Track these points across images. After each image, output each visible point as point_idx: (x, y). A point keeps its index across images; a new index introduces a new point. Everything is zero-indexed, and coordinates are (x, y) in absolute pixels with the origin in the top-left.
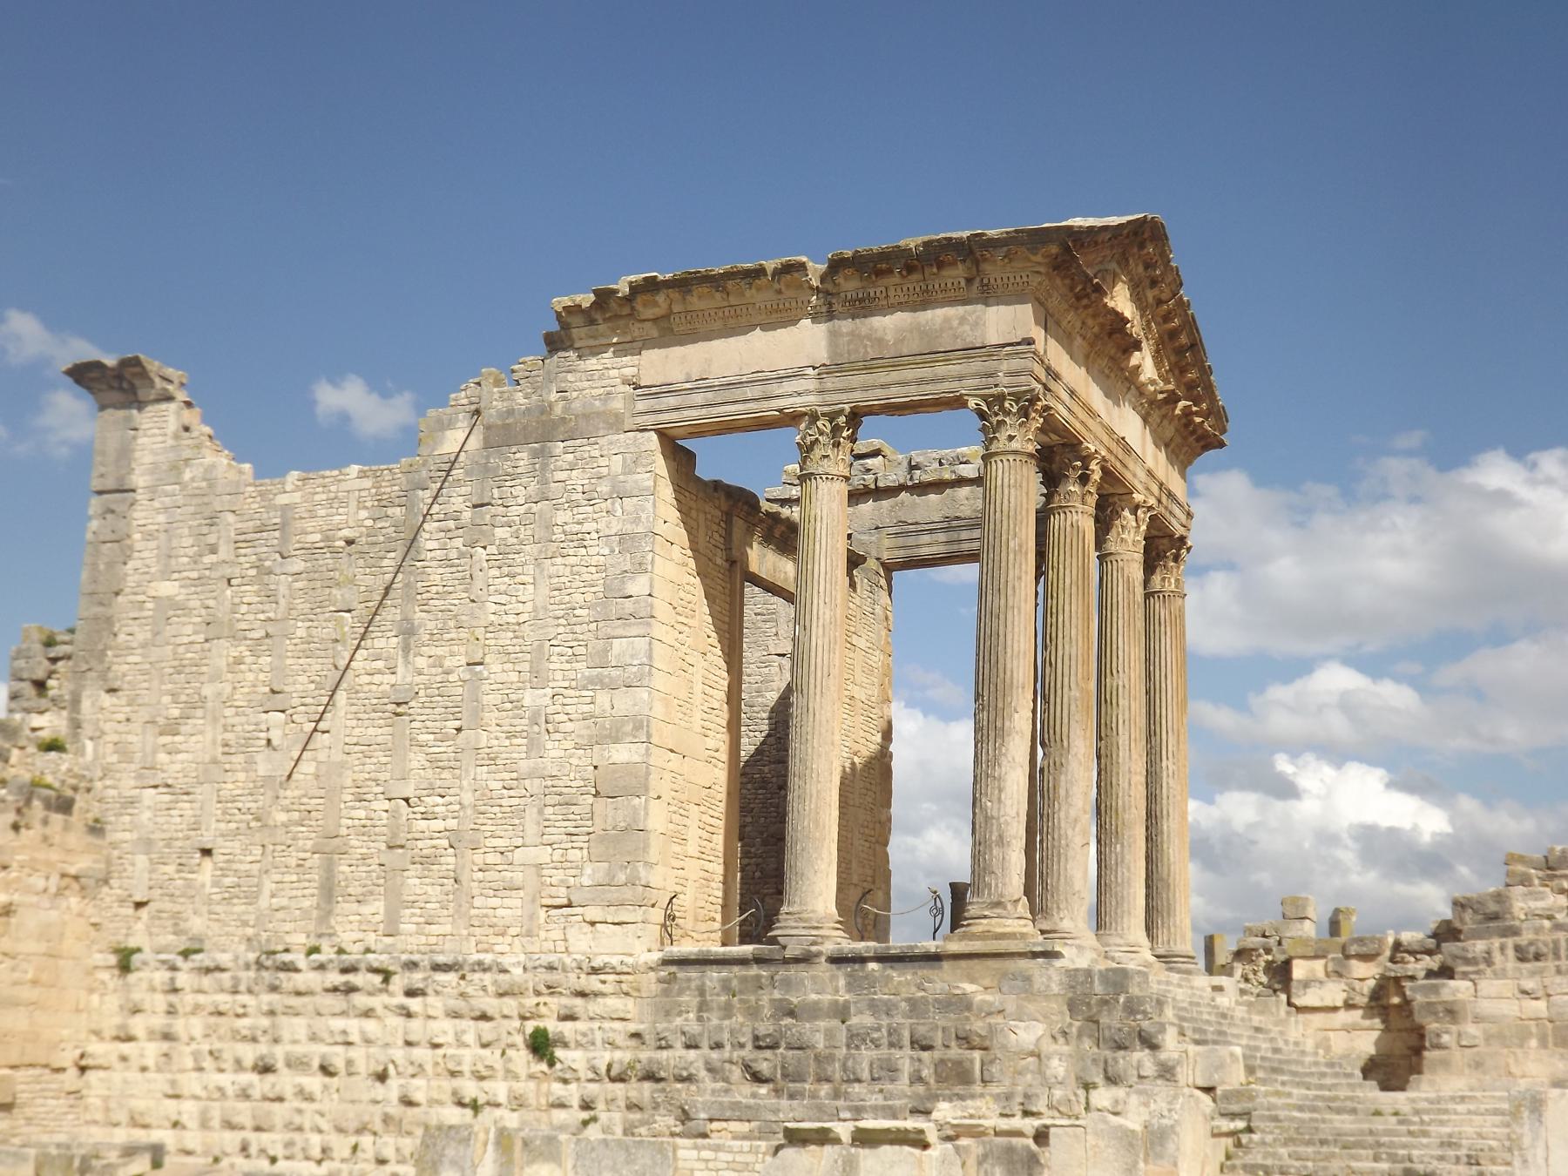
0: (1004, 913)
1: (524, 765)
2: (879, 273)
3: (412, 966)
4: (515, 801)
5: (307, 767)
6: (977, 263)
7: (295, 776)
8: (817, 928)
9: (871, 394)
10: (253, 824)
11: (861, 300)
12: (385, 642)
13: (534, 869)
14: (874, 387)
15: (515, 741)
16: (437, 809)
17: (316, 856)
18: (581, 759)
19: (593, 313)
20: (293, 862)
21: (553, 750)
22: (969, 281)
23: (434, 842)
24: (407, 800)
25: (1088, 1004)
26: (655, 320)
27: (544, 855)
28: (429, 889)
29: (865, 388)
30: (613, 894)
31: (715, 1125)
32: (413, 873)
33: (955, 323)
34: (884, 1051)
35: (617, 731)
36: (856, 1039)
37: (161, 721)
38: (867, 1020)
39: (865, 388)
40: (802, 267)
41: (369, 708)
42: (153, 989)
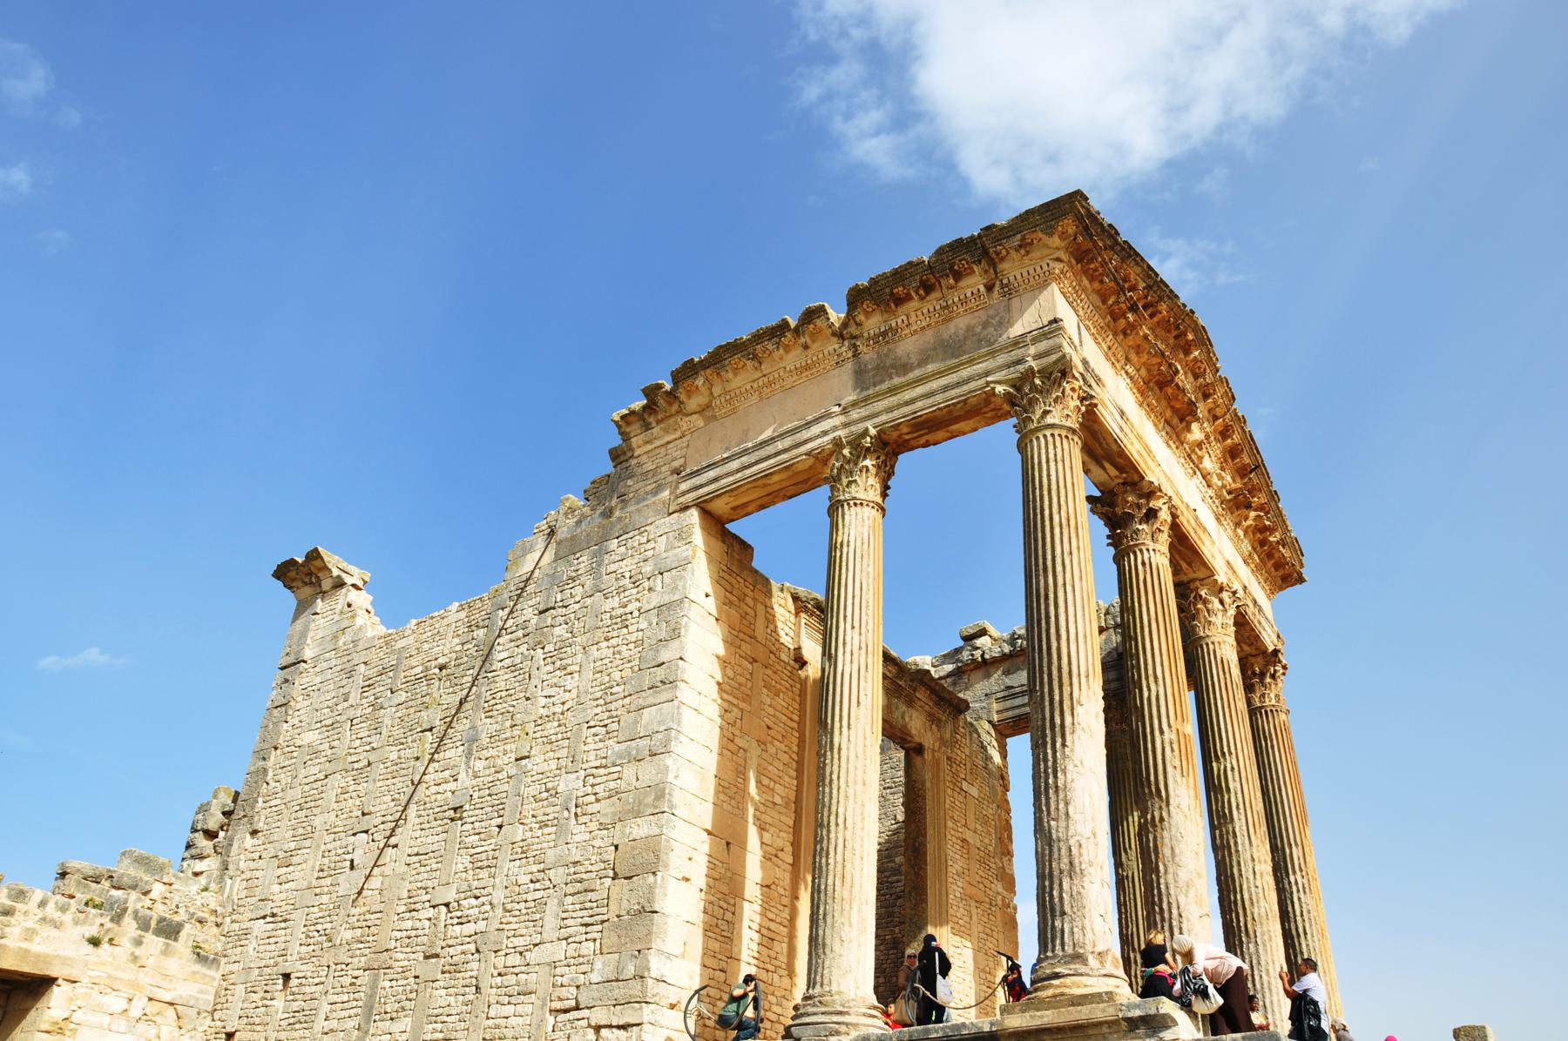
0: (1082, 969)
1: (551, 855)
2: (900, 301)
4: (538, 895)
5: (375, 883)
6: (993, 264)
7: (365, 893)
8: (841, 1013)
9: (896, 414)
10: (325, 945)
11: (884, 334)
12: (453, 754)
13: (547, 968)
14: (899, 406)
15: (546, 830)
16: (471, 912)
17: (367, 972)
18: (603, 840)
19: (646, 416)
20: (347, 980)
21: (579, 833)
22: (989, 288)
23: (464, 947)
24: (447, 905)
26: (701, 411)
27: (559, 951)
28: (452, 999)
29: (889, 410)
30: (619, 991)
32: (442, 984)
33: (978, 330)
35: (640, 803)
37: (281, 855)
39: (889, 410)
40: (821, 311)
41: (431, 818)
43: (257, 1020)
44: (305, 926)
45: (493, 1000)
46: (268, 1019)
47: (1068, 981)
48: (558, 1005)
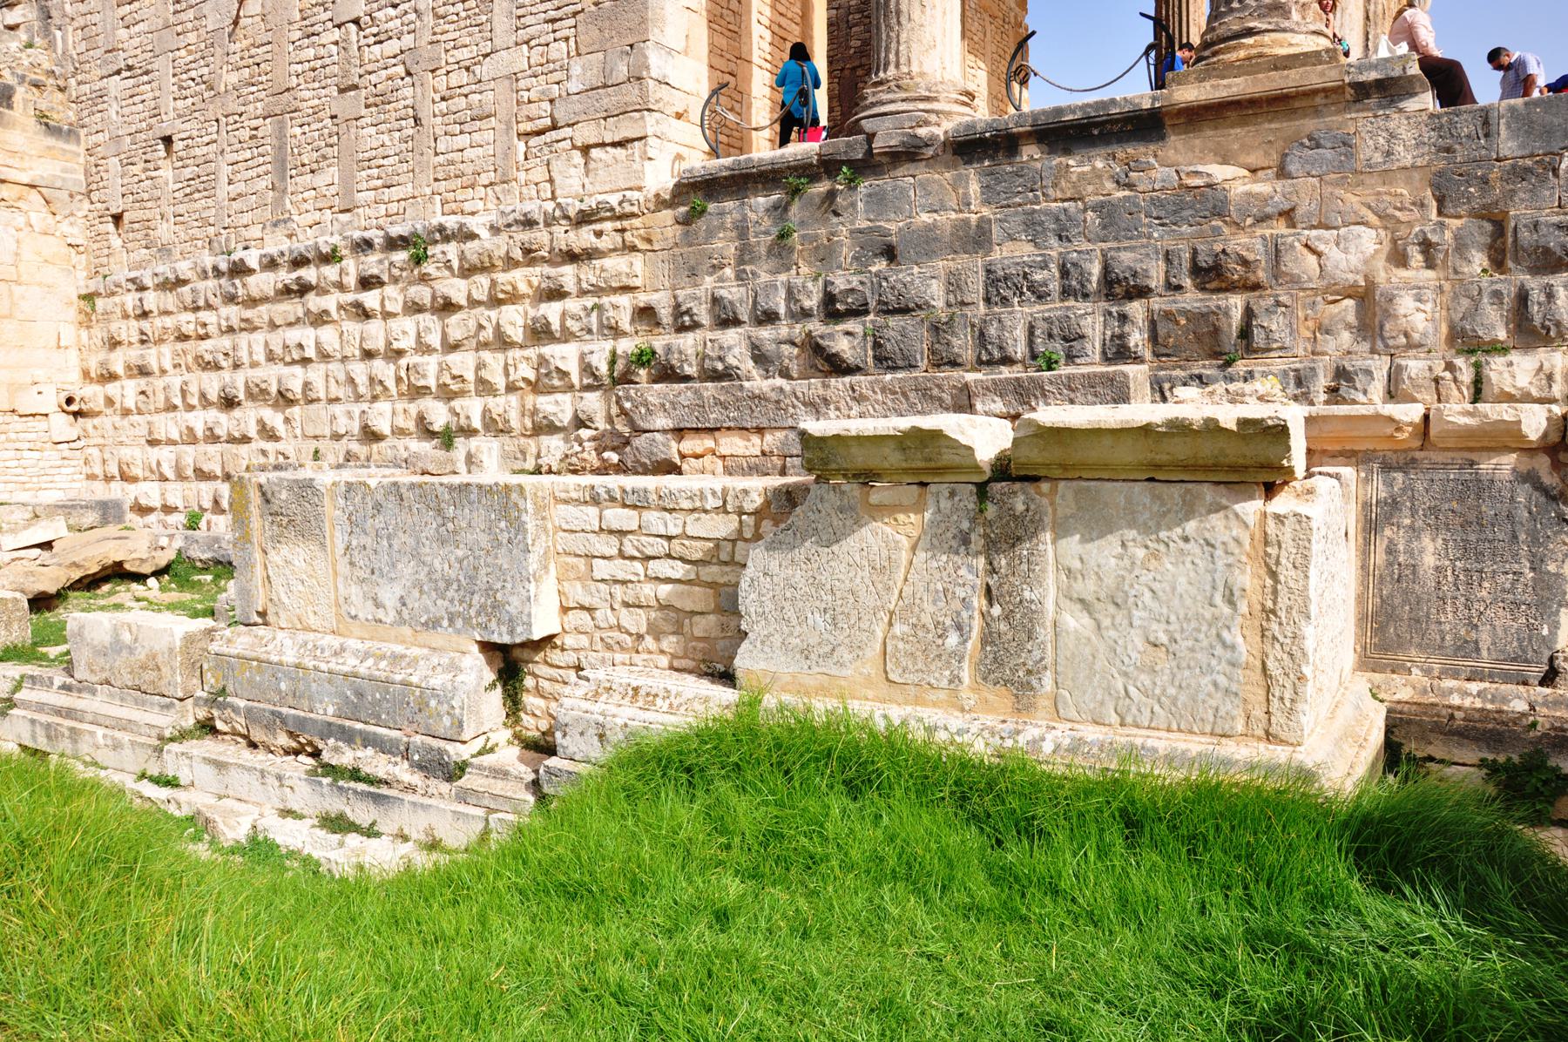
3: (366, 245)
7: (243, 22)
8: (927, 99)
10: (206, 95)
13: (507, 82)
16: (391, 25)
17: (269, 120)
20: (245, 134)
23: (391, 71)
24: (356, 22)
25: (1485, 181)
27: (519, 59)
28: (385, 138)
30: (609, 100)
31: (690, 444)
32: (369, 120)
34: (1054, 307)
36: (999, 287)
38: (1024, 251)
42: (126, 316)
43: (146, 196)
44: (174, 75)
45: (439, 131)
46: (157, 193)
47: (1267, 38)
48: (527, 127)
